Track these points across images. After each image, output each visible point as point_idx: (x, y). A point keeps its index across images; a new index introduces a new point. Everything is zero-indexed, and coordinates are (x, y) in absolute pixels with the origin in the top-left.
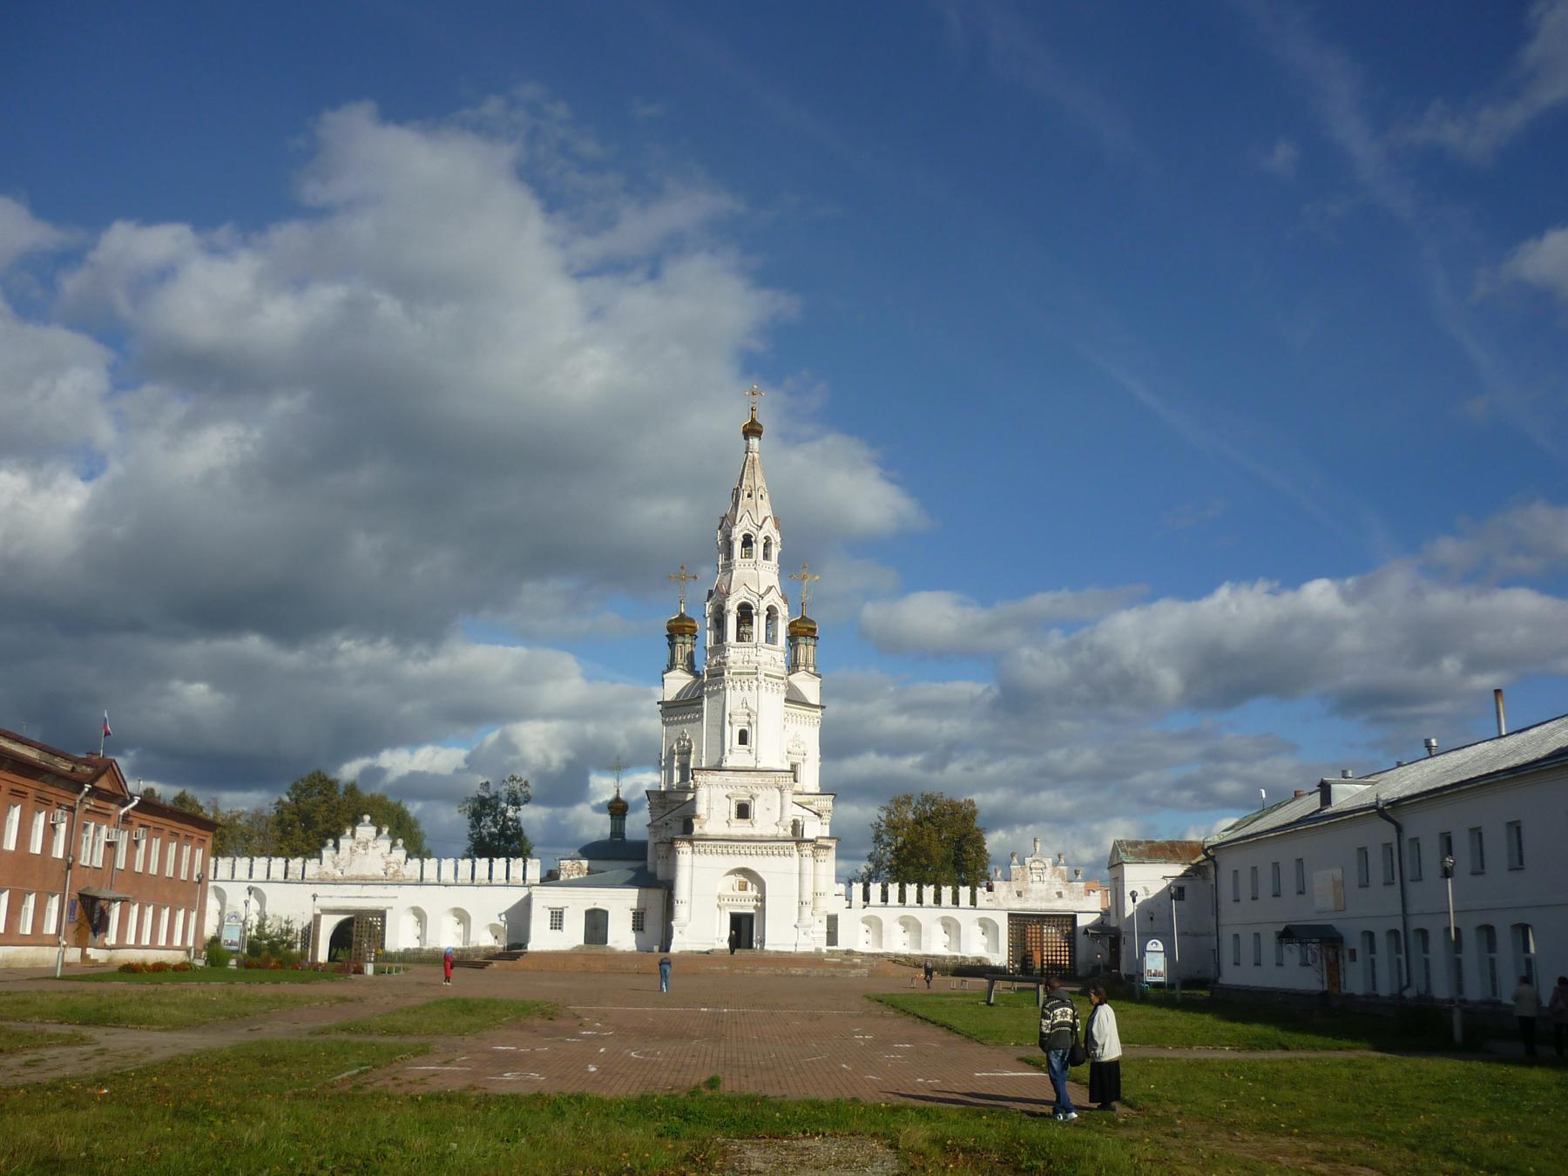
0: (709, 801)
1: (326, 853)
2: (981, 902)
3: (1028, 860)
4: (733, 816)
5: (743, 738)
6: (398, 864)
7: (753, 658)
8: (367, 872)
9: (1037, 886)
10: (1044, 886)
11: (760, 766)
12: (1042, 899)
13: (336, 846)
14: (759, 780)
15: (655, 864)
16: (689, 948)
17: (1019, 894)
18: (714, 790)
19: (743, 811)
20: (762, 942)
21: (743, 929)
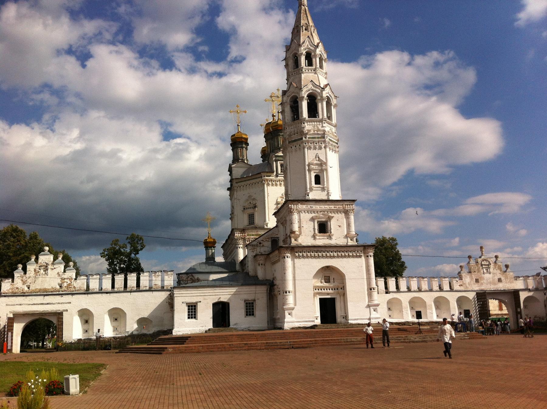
0: (300, 222)
1: (18, 274)
2: (456, 287)
3: (480, 260)
4: (317, 231)
5: (318, 180)
6: (70, 279)
7: (320, 127)
8: (47, 286)
9: (487, 276)
10: (491, 275)
11: (331, 198)
12: (490, 283)
13: (25, 269)
14: (332, 207)
15: (255, 271)
16: (297, 325)
17: (477, 281)
18: (303, 215)
19: (323, 228)
20: (346, 317)
21: (328, 308)
